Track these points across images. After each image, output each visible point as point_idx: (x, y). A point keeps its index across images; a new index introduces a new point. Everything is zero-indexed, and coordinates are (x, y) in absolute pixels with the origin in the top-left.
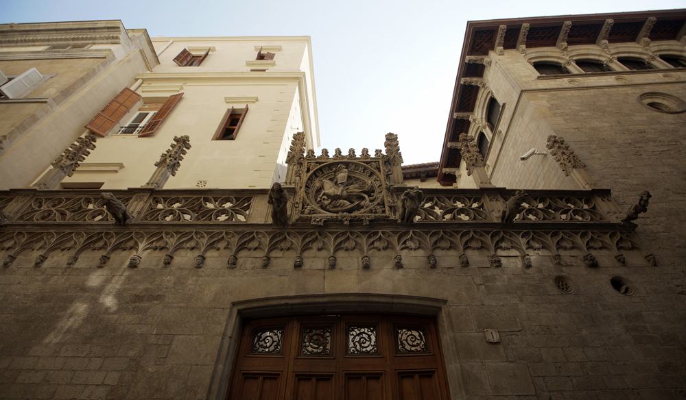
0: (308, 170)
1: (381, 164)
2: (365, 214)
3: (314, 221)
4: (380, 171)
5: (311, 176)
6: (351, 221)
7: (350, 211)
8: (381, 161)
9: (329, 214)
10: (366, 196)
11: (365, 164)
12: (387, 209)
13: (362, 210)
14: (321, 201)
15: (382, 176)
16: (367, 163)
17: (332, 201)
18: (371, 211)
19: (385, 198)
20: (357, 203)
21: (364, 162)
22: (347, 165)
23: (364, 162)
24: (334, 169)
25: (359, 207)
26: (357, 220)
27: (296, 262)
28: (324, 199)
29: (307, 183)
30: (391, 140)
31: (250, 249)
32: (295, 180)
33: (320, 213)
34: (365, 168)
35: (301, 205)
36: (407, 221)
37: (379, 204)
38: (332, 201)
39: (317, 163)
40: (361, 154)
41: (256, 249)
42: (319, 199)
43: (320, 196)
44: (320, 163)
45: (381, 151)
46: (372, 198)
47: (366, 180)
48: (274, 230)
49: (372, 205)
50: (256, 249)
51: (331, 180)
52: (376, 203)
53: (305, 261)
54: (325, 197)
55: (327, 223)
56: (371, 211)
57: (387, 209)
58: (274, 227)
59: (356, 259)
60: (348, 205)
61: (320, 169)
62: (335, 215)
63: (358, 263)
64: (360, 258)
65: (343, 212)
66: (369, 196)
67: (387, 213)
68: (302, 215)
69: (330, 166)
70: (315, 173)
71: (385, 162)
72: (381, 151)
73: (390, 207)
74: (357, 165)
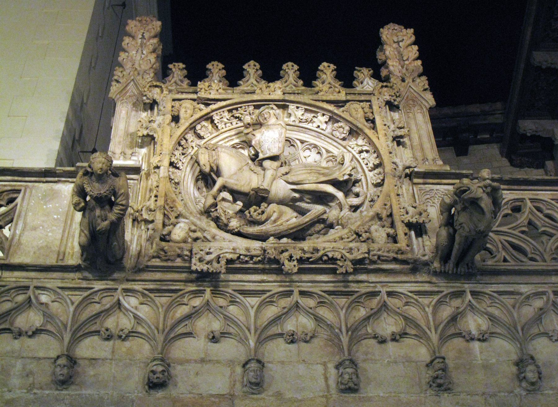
0: (176, 119)
1: (375, 107)
3: (201, 260)
7: (298, 234)
12: (401, 229)
13: (332, 234)
17: (247, 206)
27: (153, 372)
31: (20, 334)
35: (159, 217)
36: (457, 265)
38: (247, 206)
41: (37, 332)
46: (355, 201)
48: (84, 284)
49: (356, 221)
50: (37, 332)
52: (367, 212)
53: (177, 370)
54: (226, 195)
55: (235, 265)
58: (86, 274)
59: (320, 368)
60: (290, 219)
62: (257, 245)
63: (326, 379)
64: (331, 366)
65: (279, 236)
67: (402, 243)
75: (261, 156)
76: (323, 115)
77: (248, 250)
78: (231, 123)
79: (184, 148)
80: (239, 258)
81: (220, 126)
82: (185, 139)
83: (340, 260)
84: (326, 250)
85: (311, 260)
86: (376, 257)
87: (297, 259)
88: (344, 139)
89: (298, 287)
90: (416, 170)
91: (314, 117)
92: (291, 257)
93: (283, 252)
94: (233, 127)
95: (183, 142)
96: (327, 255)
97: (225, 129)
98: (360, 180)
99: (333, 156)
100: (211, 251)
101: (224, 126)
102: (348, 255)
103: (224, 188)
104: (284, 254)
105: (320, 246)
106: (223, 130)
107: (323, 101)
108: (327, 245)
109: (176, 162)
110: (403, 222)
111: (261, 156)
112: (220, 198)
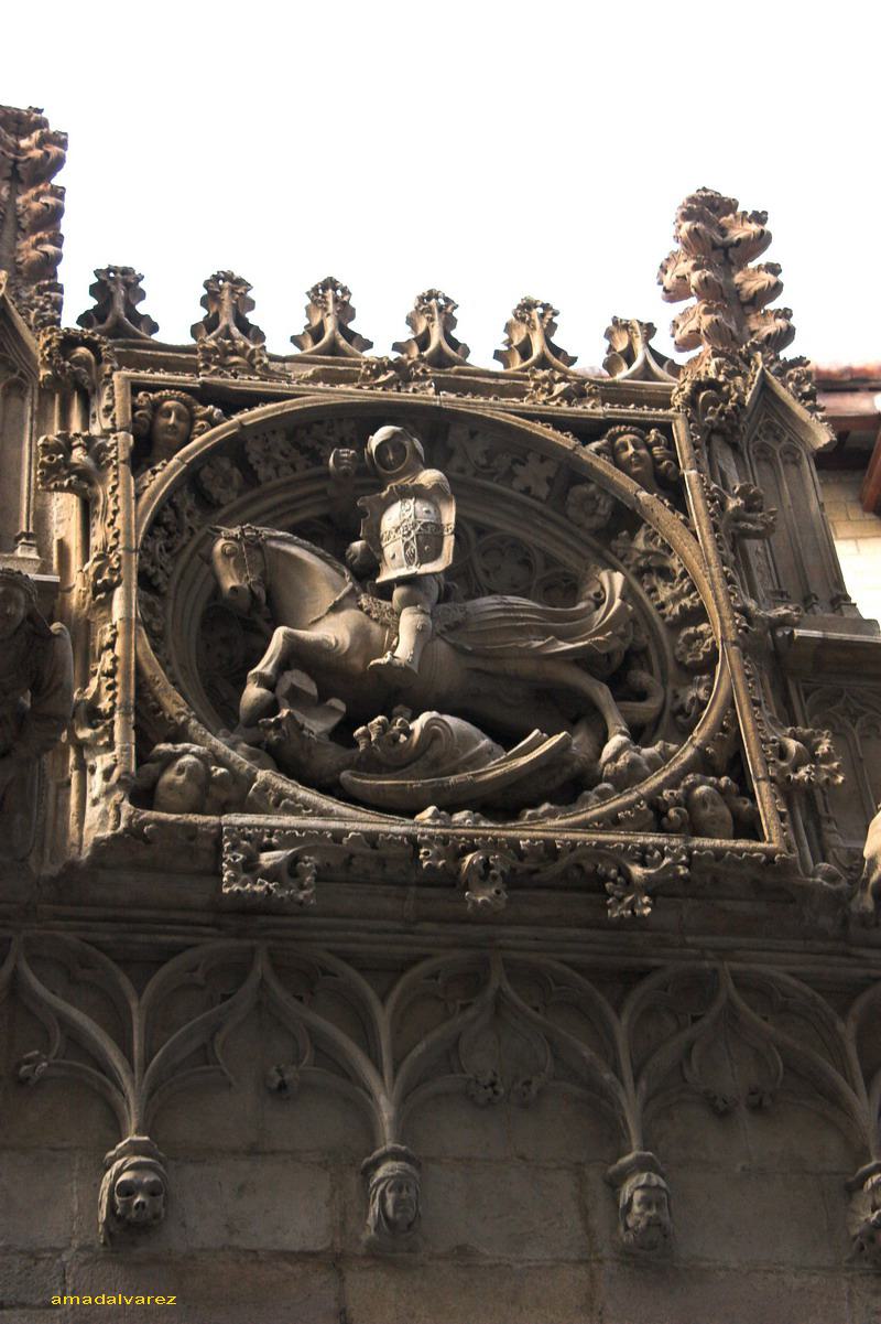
2: (616, 838)
4: (679, 503)
5: (169, 502)
6: (513, 881)
7: (504, 802)
8: (680, 430)
9: (359, 822)
10: (603, 694)
11: (567, 441)
12: (766, 802)
14: (273, 708)
15: (694, 547)
16: (587, 430)
18: (656, 815)
19: (746, 723)
20: (542, 745)
21: (560, 423)
22: (436, 433)
23: (560, 423)
24: (337, 458)
25: (567, 783)
26: (564, 884)
28: (295, 696)
29: (144, 551)
30: (721, 247)
32: (41, 517)
33: (281, 804)
34: (573, 474)
37: (703, 764)
39: (206, 394)
40: (498, 341)
42: (253, 692)
43: (265, 666)
44: (233, 402)
45: (650, 330)
47: (572, 562)
51: (334, 548)
54: (297, 678)
56: (656, 815)
57: (766, 802)
61: (233, 448)
66: (626, 691)
67: (773, 837)
68: (147, 814)
69: (310, 432)
70: (192, 478)
71: (711, 432)
72: (650, 330)
73: (786, 790)
74: (512, 445)
75: (387, 575)
76: (543, 459)
77: (372, 839)
78: (293, 467)
79: (170, 534)
80: (348, 863)
81: (263, 471)
82: (173, 505)
83: (614, 881)
84: (577, 852)
85: (536, 877)
86: (708, 879)
87: (502, 873)
88: (597, 533)
89: (501, 948)
90: (798, 632)
91: (515, 461)
92: (486, 865)
93: (465, 852)
94: (297, 475)
95: (168, 516)
96: (579, 867)
97: (277, 482)
98: (645, 651)
99: (565, 574)
100: (274, 840)
101: (271, 472)
102: (637, 871)
103: (296, 655)
104: (468, 858)
105: (561, 839)
106: (270, 485)
107: (543, 419)
108: (579, 836)
109: (152, 570)
110: (772, 780)
111: (387, 575)
112: (283, 687)
